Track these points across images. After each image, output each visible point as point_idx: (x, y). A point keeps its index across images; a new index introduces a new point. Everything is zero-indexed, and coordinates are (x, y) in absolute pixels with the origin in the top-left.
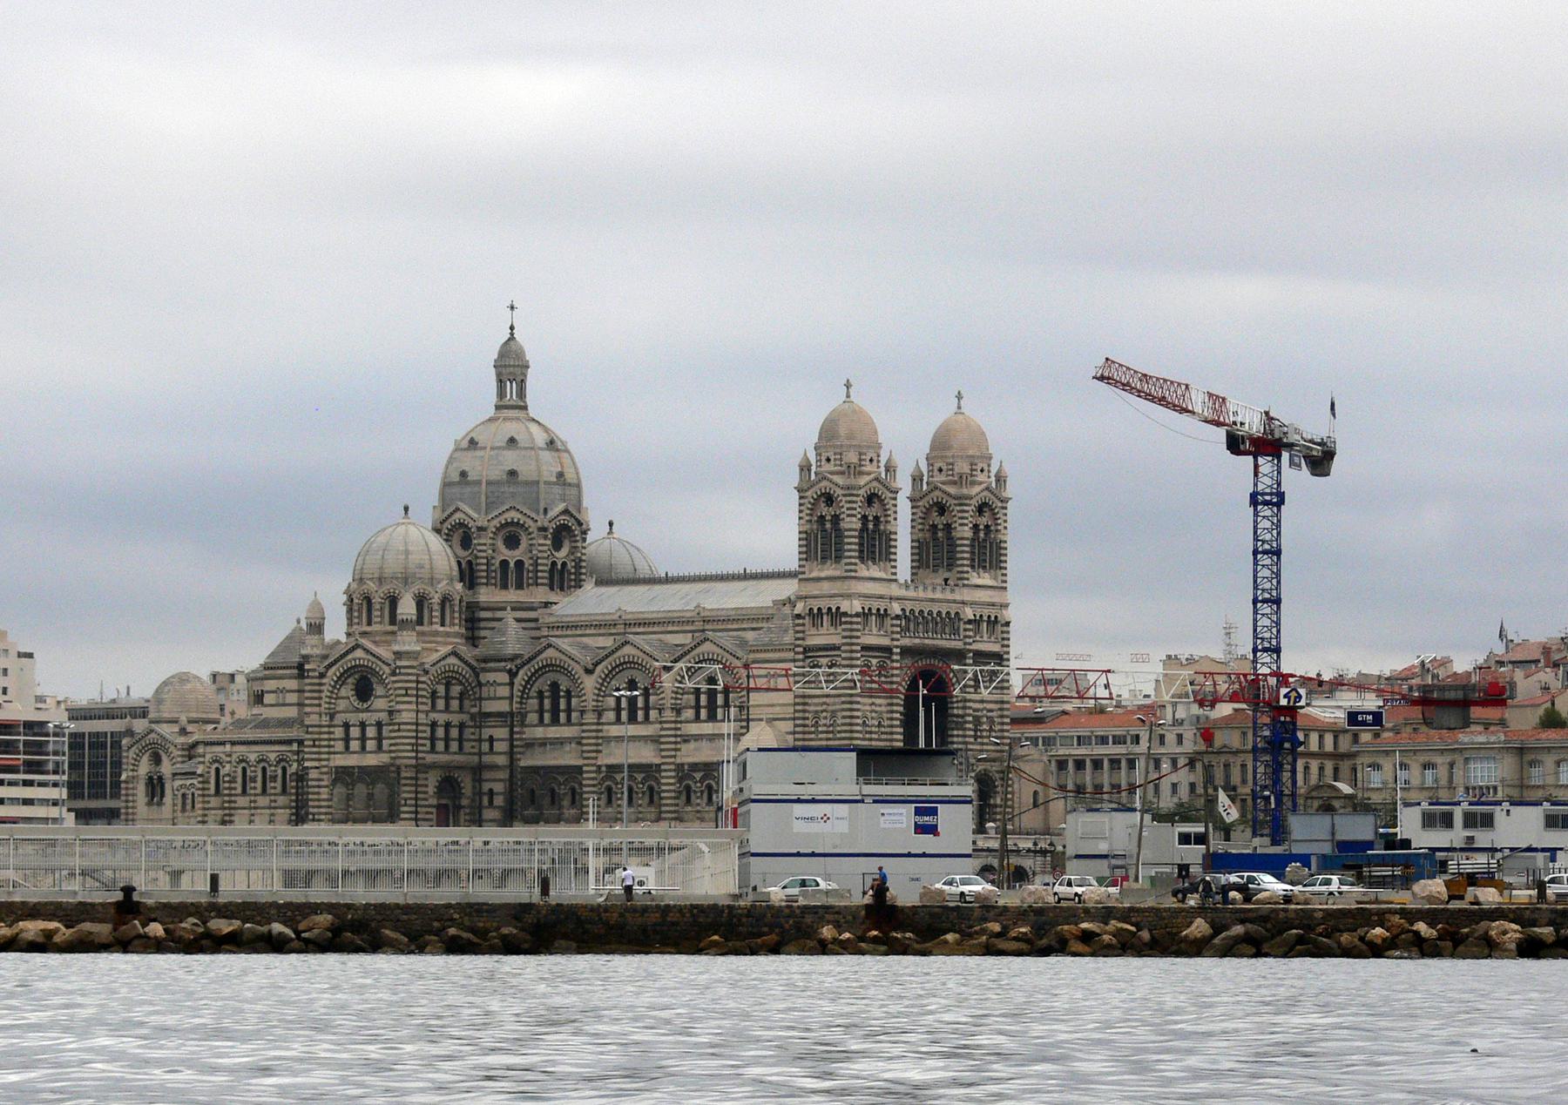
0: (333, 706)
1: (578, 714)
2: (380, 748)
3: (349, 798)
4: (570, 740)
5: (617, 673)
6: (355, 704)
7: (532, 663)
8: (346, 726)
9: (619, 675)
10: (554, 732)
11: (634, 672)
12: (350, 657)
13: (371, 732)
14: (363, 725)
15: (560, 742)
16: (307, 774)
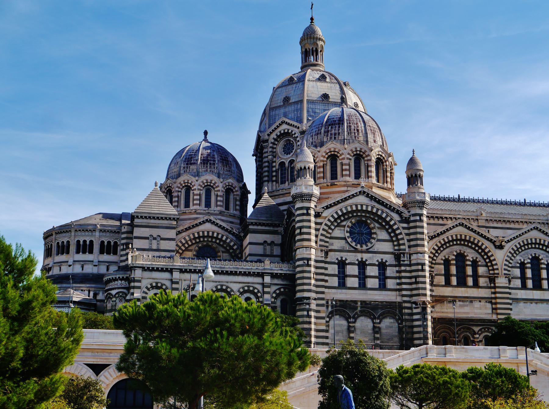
0: (327, 244)
1: (487, 280)
2: (383, 287)
3: (350, 330)
4: (480, 299)
5: (522, 251)
6: (353, 244)
7: (442, 237)
8: (342, 264)
9: (523, 253)
10: (461, 292)
11: (538, 252)
12: (350, 202)
13: (372, 271)
14: (362, 265)
15: (471, 299)
16: (309, 304)
